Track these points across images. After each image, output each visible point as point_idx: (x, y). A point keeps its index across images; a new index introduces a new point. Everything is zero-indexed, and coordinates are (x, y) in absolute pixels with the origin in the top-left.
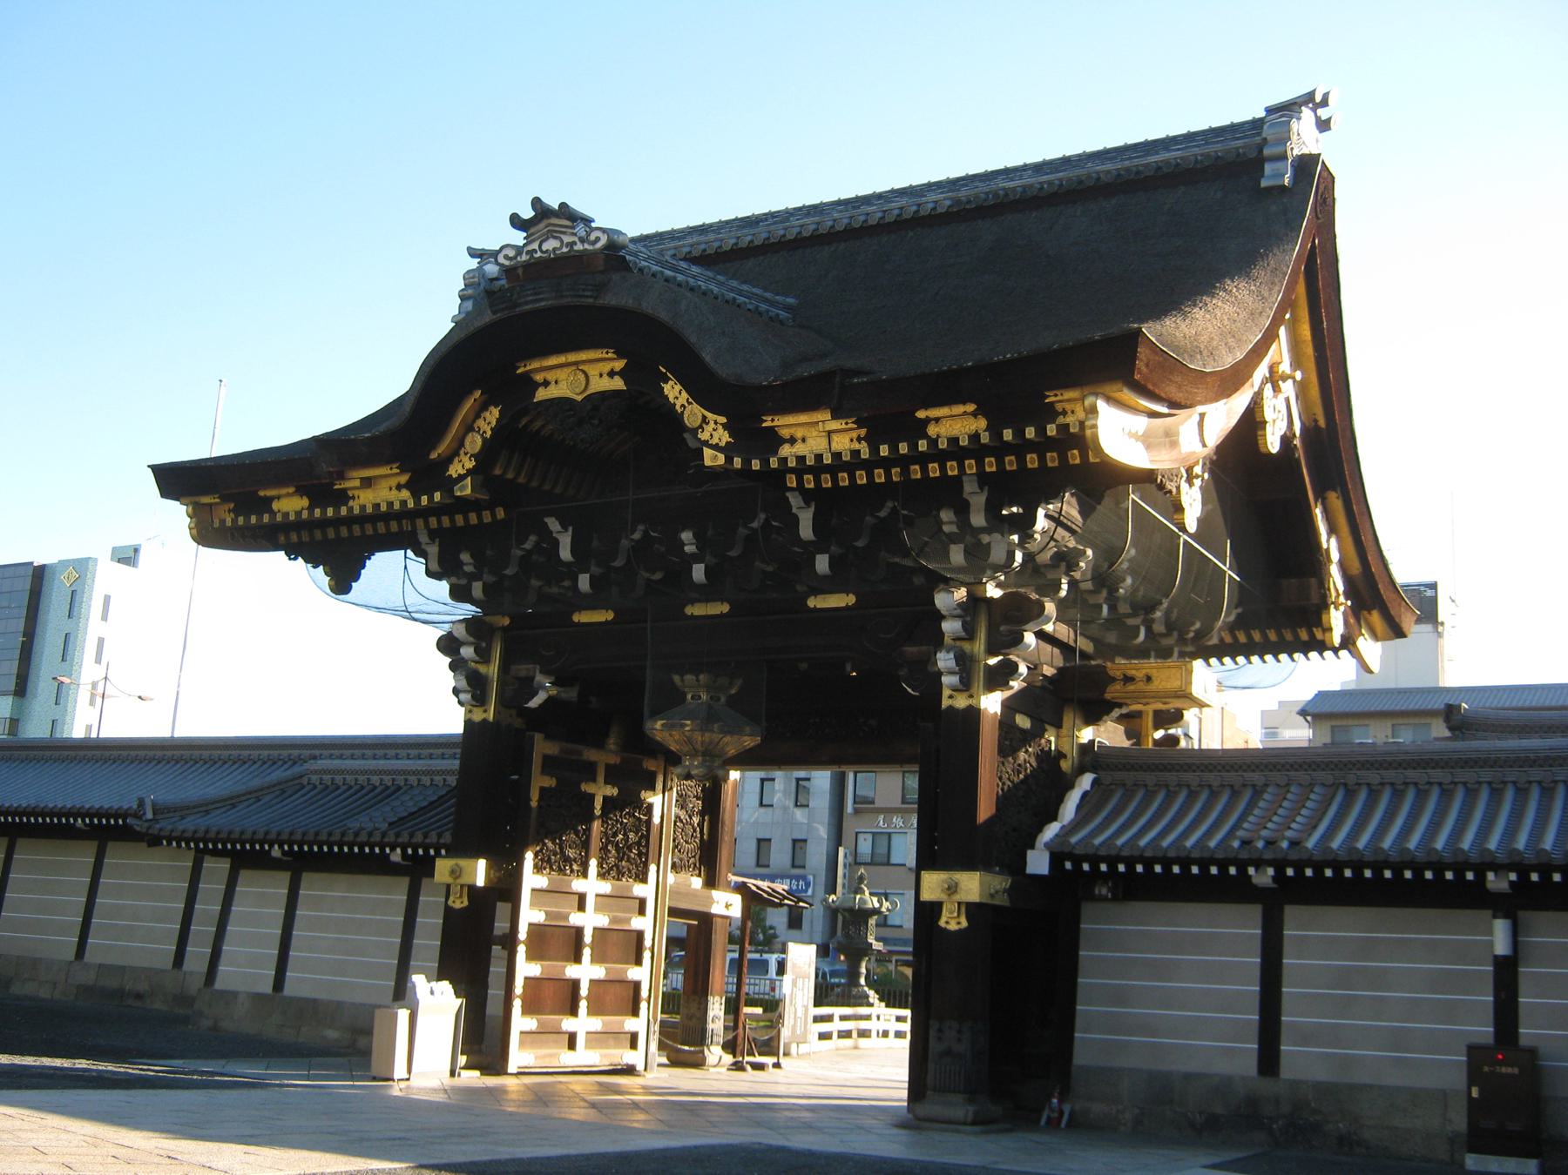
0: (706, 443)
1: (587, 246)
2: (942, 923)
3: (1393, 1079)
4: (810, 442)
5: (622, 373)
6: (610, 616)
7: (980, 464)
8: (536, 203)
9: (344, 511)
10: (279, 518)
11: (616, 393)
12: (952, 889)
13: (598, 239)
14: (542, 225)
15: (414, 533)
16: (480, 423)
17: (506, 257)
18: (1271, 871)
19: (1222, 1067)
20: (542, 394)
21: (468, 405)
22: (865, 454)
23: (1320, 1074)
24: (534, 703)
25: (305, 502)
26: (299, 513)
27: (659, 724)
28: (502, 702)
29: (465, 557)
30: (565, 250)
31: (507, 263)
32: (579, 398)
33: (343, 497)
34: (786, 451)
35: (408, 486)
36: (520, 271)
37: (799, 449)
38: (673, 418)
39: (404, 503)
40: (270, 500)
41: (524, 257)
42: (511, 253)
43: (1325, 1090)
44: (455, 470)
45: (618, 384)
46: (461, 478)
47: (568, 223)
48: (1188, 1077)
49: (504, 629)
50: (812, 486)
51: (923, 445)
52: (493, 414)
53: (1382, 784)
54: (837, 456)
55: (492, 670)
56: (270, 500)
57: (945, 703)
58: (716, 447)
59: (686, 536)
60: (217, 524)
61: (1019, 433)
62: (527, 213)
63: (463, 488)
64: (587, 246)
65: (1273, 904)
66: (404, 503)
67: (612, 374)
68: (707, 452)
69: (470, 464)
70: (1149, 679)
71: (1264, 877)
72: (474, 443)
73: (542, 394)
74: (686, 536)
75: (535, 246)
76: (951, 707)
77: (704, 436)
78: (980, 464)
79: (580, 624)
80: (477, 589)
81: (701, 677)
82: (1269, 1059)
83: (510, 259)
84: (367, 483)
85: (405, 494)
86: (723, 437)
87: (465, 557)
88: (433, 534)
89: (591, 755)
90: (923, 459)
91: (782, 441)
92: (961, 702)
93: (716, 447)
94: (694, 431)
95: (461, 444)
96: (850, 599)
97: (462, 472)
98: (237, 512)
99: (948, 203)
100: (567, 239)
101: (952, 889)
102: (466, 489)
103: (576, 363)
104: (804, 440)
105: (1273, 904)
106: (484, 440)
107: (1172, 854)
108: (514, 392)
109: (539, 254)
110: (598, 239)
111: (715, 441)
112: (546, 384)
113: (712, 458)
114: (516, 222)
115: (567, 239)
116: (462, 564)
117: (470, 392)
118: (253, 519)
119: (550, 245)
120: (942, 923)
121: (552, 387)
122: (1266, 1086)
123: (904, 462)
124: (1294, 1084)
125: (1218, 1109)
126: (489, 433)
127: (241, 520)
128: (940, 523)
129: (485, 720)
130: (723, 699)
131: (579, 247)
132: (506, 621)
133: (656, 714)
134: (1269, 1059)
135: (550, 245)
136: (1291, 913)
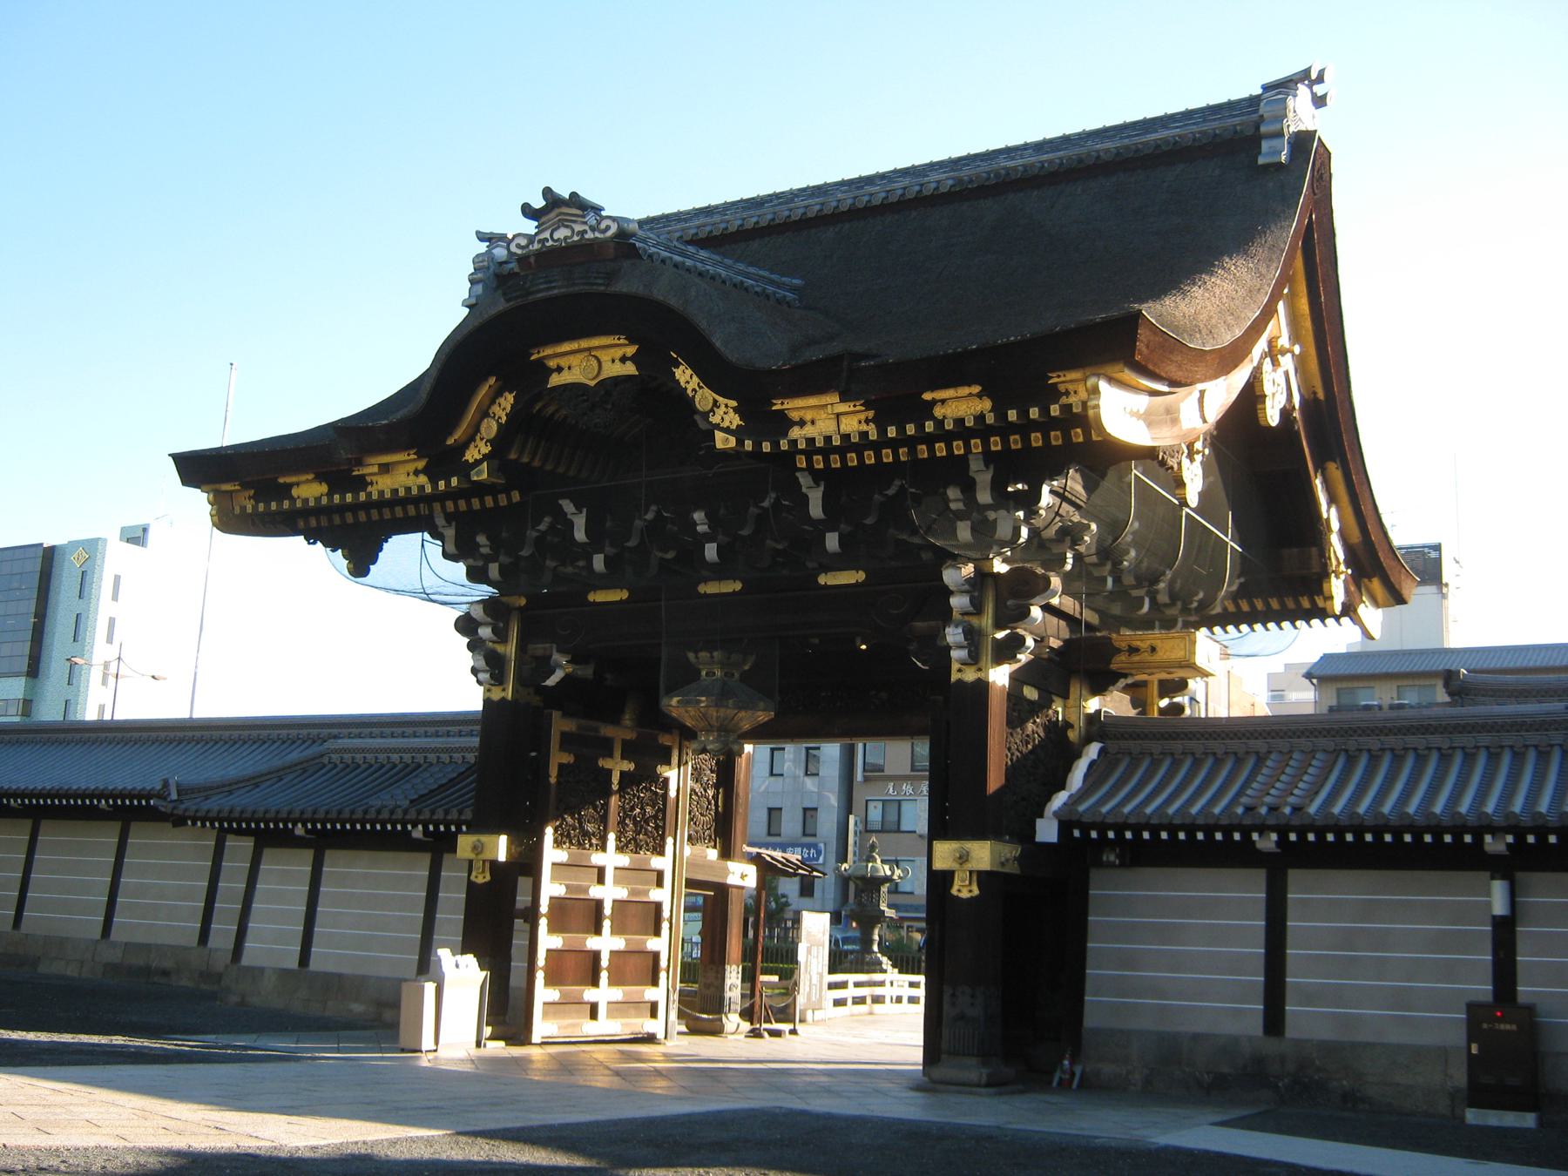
0: (717, 427)
1: (597, 235)
2: (954, 891)
3: (1394, 1037)
5: (633, 359)
6: (625, 595)
7: (986, 444)
8: (547, 192)
9: (362, 497)
10: (299, 504)
11: (629, 378)
12: (963, 858)
13: (608, 228)
14: (552, 215)
15: (431, 517)
16: (495, 409)
17: (518, 246)
18: (1274, 836)
19: (1230, 1028)
20: (555, 380)
21: (483, 391)
22: (873, 436)
23: (1326, 1033)
24: (551, 681)
25: (324, 488)
26: (318, 499)
27: (674, 701)
28: (520, 681)
29: (481, 539)
30: (576, 238)
31: (519, 252)
32: (592, 383)
33: (362, 483)
34: (795, 433)
36: (532, 260)
38: (683, 401)
39: (421, 488)
40: (290, 486)
41: (536, 246)
42: (523, 242)
43: (1329, 1049)
44: (471, 455)
45: (630, 369)
46: (478, 463)
47: (579, 212)
48: (1196, 1037)
49: (520, 609)
50: (821, 466)
51: (929, 426)
52: (508, 400)
53: (1383, 750)
54: (846, 437)
55: (510, 650)
56: (290, 486)
57: (954, 677)
58: (727, 430)
59: (698, 516)
60: (237, 510)
61: (1024, 413)
62: (538, 203)
63: (478, 474)
64: (597, 235)
65: (1277, 868)
66: (421, 488)
67: (623, 359)
68: (719, 435)
69: (486, 450)
70: (1153, 649)
71: (1267, 842)
72: (490, 428)
73: (555, 380)
74: (698, 516)
75: (547, 235)
76: (960, 681)
77: (715, 419)
78: (986, 444)
79: (595, 604)
80: (494, 570)
81: (715, 654)
82: (1274, 1020)
83: (522, 248)
84: (385, 469)
85: (423, 479)
86: (734, 420)
87: (481, 539)
88: (449, 518)
89: (607, 731)
90: (930, 440)
91: (792, 424)
92: (970, 676)
93: (727, 430)
94: (705, 415)
95: (478, 430)
96: (861, 576)
97: (478, 457)
98: (257, 498)
99: (950, 182)
100: (578, 228)
101: (963, 858)
102: (482, 474)
103: (589, 349)
104: (813, 422)
105: (1277, 868)
106: (500, 425)
107: (1177, 821)
108: (528, 378)
109: (550, 243)
110: (608, 228)
111: (726, 424)
112: (559, 369)
113: (723, 441)
114: (527, 211)
116: (479, 546)
117: (486, 379)
118: (274, 506)
119: (561, 233)
120: (954, 891)
121: (565, 372)
122: (1272, 1046)
123: (911, 442)
124: (1298, 1043)
125: (1225, 1070)
126: (504, 419)
127: (261, 507)
128: (946, 501)
129: (503, 699)
131: (590, 235)
132: (523, 602)
133: (670, 691)
134: (1274, 1020)
135: (561, 233)
136: (1294, 876)
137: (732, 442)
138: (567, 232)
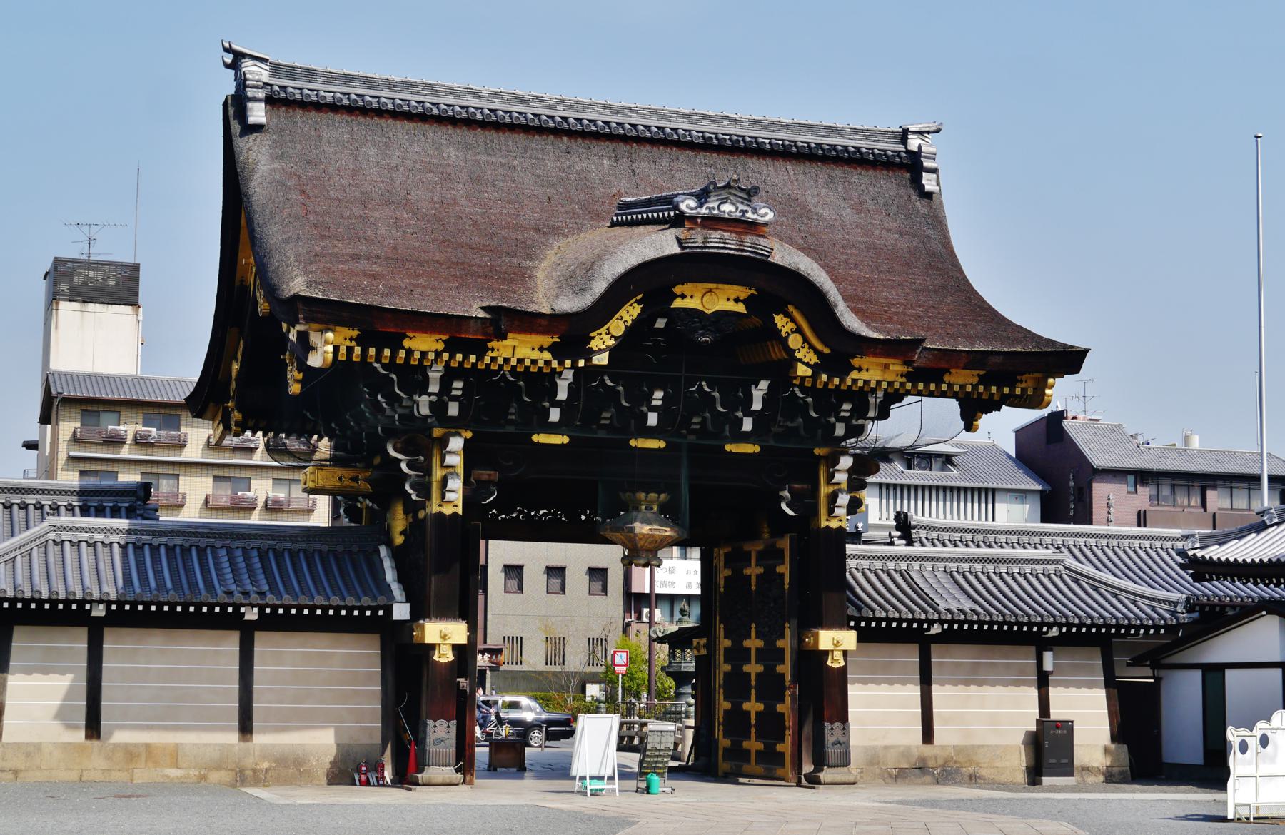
0: (800, 360)
4: (871, 372)
5: (744, 301)
6: (566, 440)
13: (766, 214)
17: (688, 206)
20: (678, 303)
34: (854, 375)
35: (551, 349)
37: (864, 375)
41: (704, 211)
43: (959, 750)
44: (594, 344)
45: (741, 308)
46: (601, 351)
48: (886, 748)
58: (807, 364)
59: (659, 394)
67: (737, 300)
68: (800, 366)
74: (659, 394)
76: (828, 527)
77: (798, 355)
81: (663, 496)
82: (928, 736)
85: (547, 356)
86: (813, 359)
91: (852, 368)
94: (794, 351)
109: (716, 212)
110: (766, 214)
111: (805, 360)
112: (683, 296)
115: (741, 207)
119: (727, 208)
124: (943, 747)
129: (455, 514)
130: (655, 508)
134: (928, 736)
136: (933, 647)
137: (809, 372)
138: (733, 209)
